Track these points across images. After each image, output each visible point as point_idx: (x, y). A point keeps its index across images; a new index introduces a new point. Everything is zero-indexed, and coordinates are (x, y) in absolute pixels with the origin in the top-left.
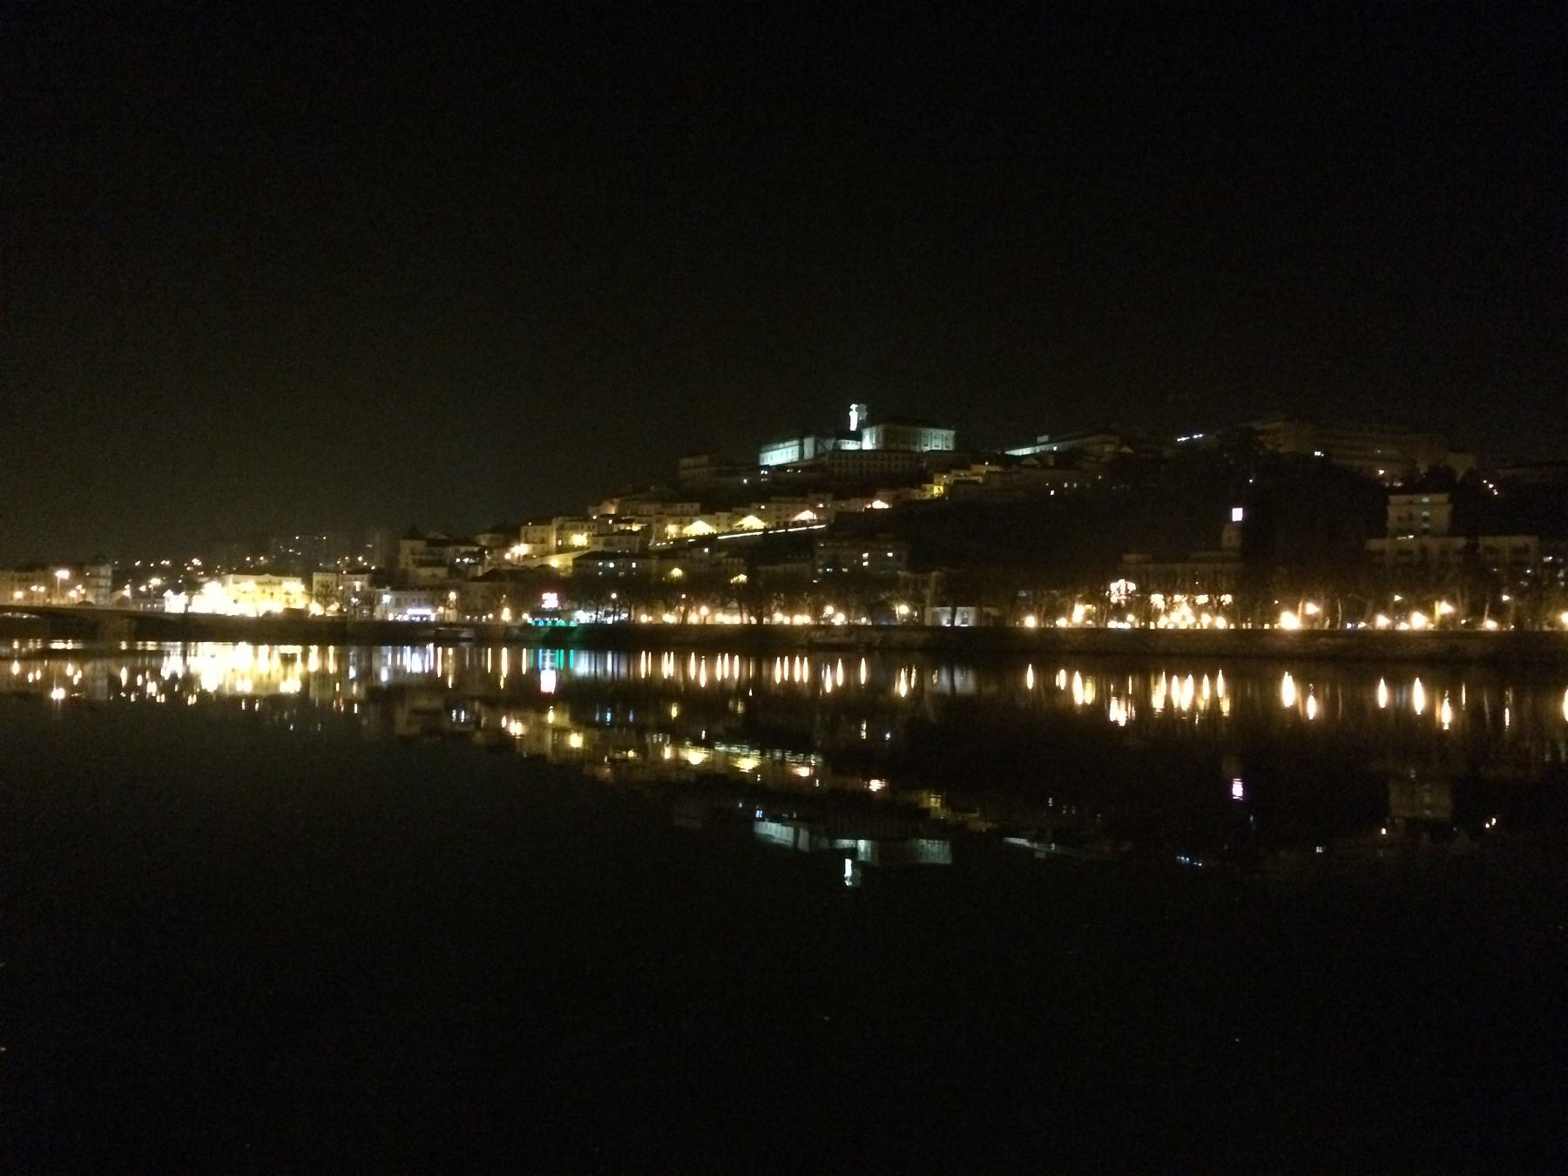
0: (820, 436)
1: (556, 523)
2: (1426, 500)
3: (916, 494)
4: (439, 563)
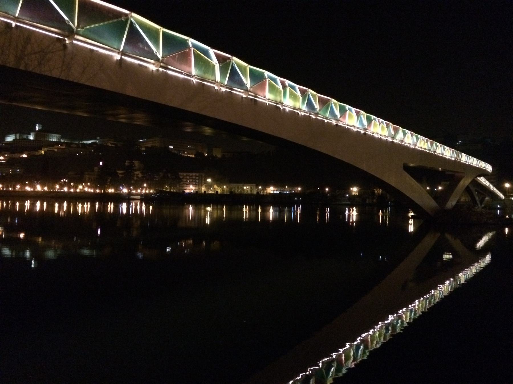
0: (21, 133)
3: (37, 153)
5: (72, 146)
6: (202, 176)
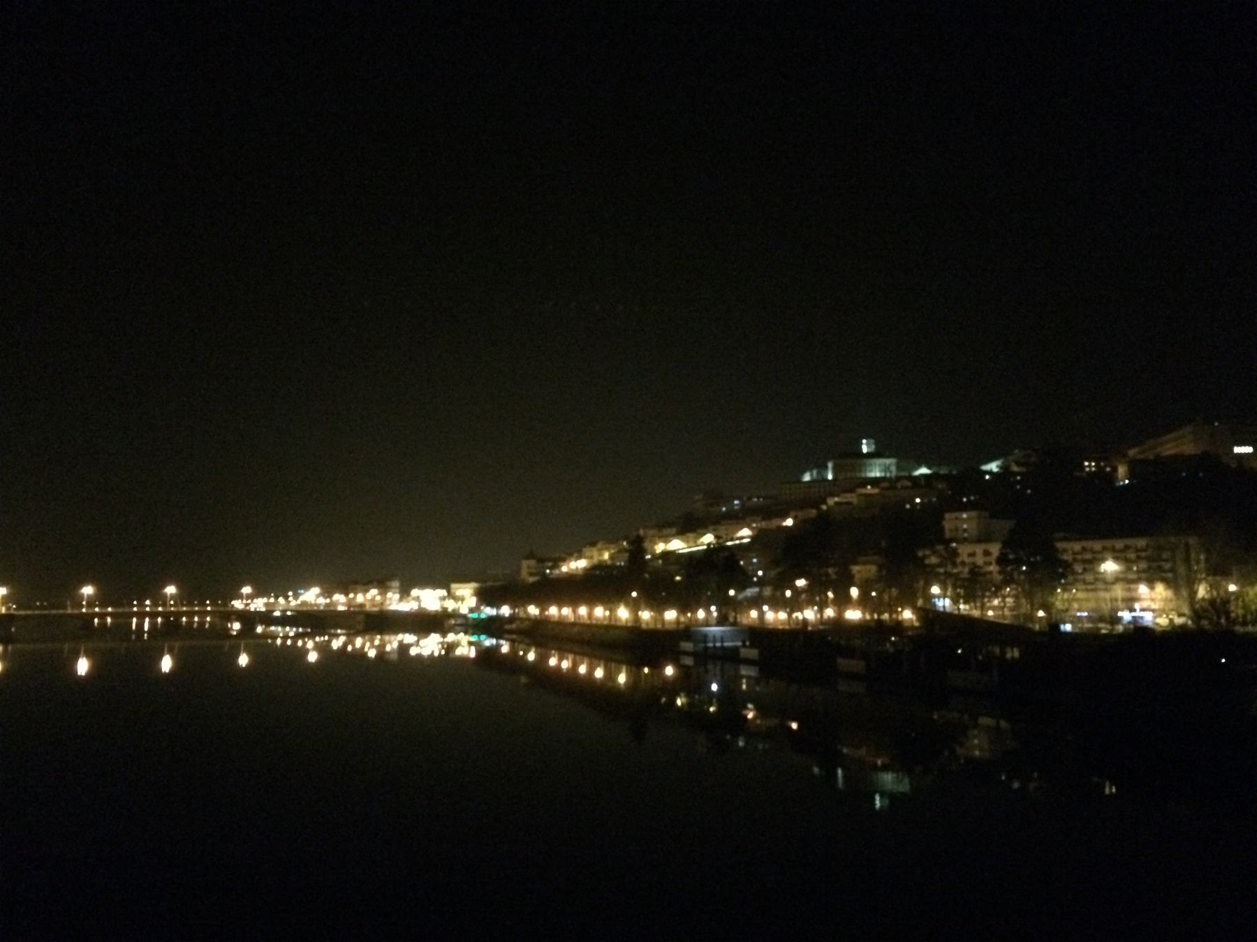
1: (600, 545)
2: (965, 516)
4: (537, 574)
5: (899, 485)
6: (1187, 546)
